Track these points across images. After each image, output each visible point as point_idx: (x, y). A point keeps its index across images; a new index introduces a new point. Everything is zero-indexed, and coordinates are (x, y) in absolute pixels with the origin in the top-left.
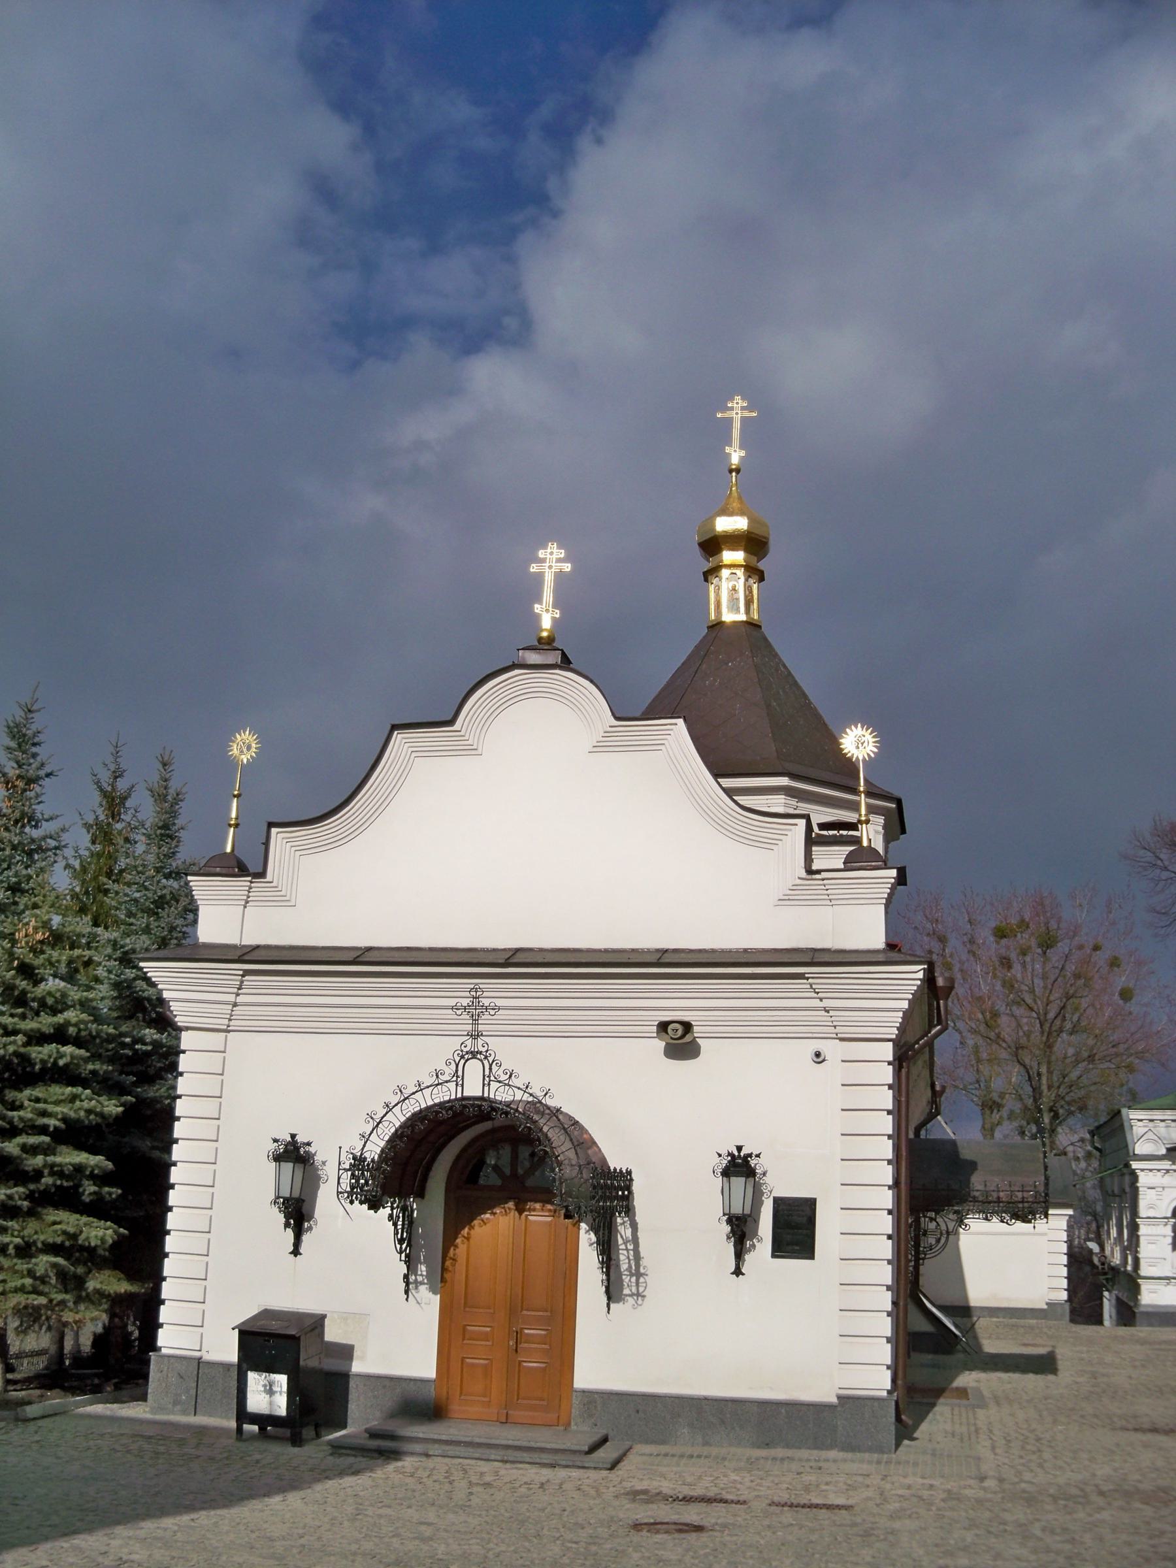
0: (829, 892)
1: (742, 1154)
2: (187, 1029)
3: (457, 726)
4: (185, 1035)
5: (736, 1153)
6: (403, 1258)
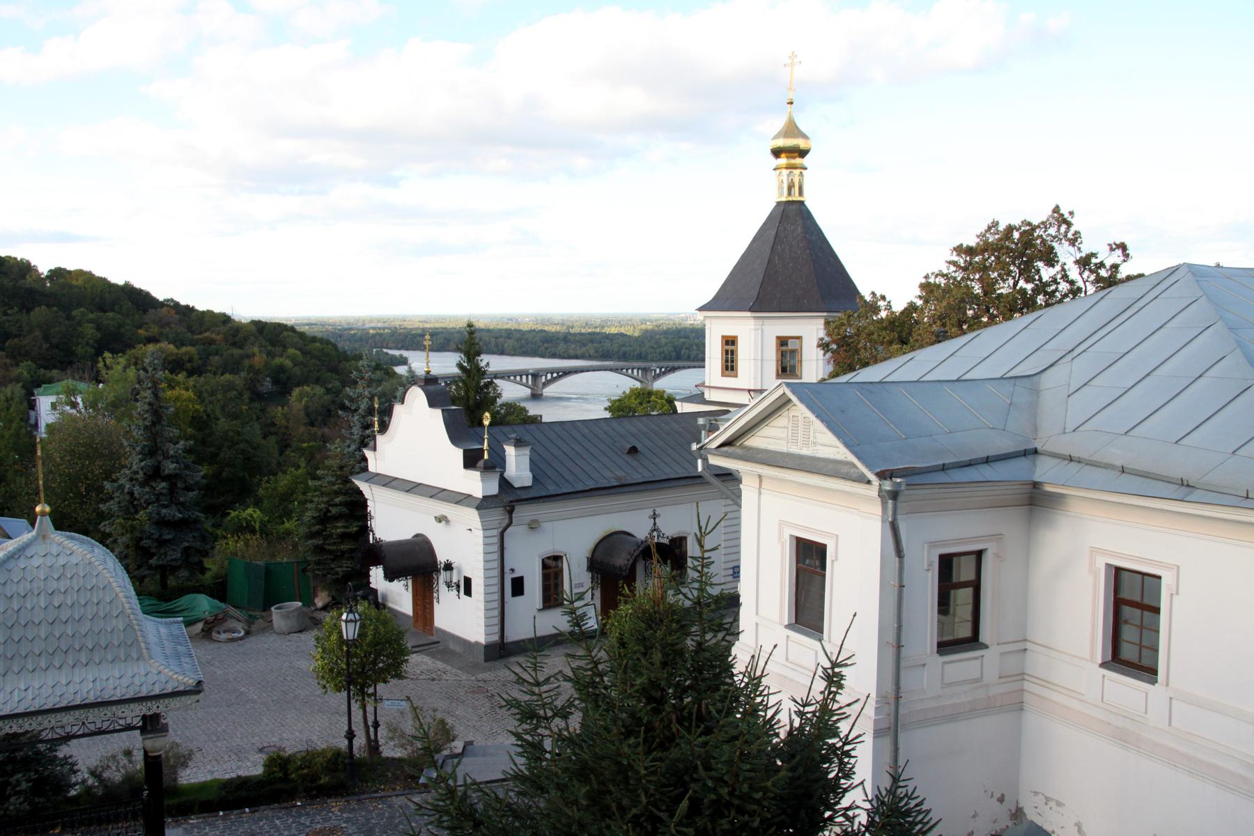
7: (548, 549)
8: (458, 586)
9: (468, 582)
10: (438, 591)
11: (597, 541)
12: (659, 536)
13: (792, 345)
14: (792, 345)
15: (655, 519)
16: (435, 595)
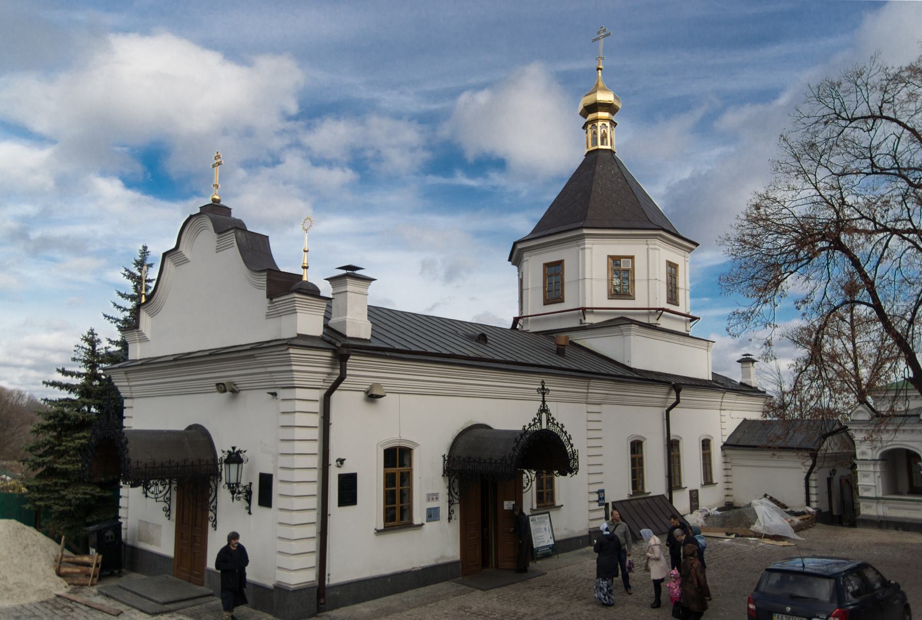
0: (279, 309)
1: (235, 451)
2: (126, 398)
3: (179, 250)
4: (125, 401)
5: (232, 451)
6: (162, 499)
7: (393, 437)
8: (249, 493)
9: (266, 481)
10: (215, 507)
11: (456, 434)
12: (548, 420)
13: (624, 264)
14: (624, 264)
15: (543, 394)
16: (211, 514)
